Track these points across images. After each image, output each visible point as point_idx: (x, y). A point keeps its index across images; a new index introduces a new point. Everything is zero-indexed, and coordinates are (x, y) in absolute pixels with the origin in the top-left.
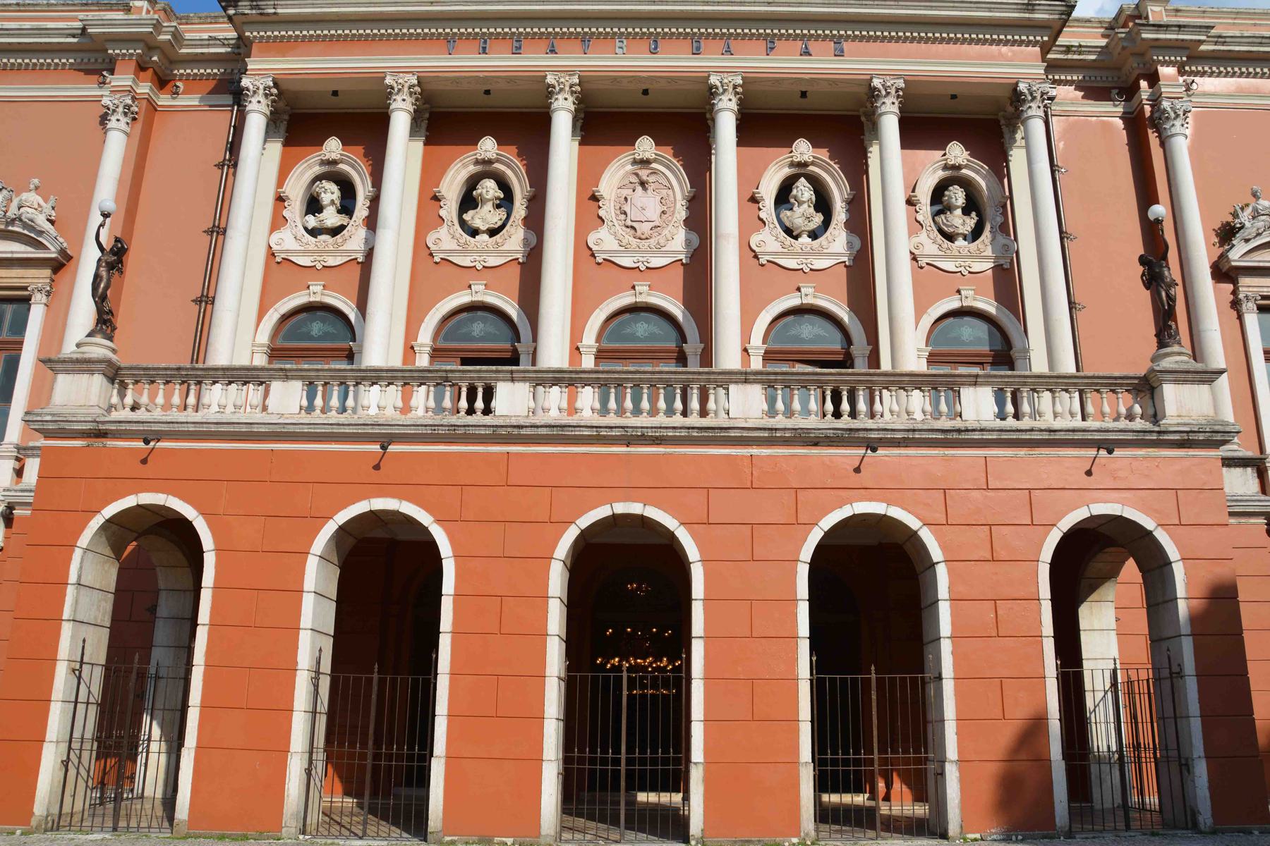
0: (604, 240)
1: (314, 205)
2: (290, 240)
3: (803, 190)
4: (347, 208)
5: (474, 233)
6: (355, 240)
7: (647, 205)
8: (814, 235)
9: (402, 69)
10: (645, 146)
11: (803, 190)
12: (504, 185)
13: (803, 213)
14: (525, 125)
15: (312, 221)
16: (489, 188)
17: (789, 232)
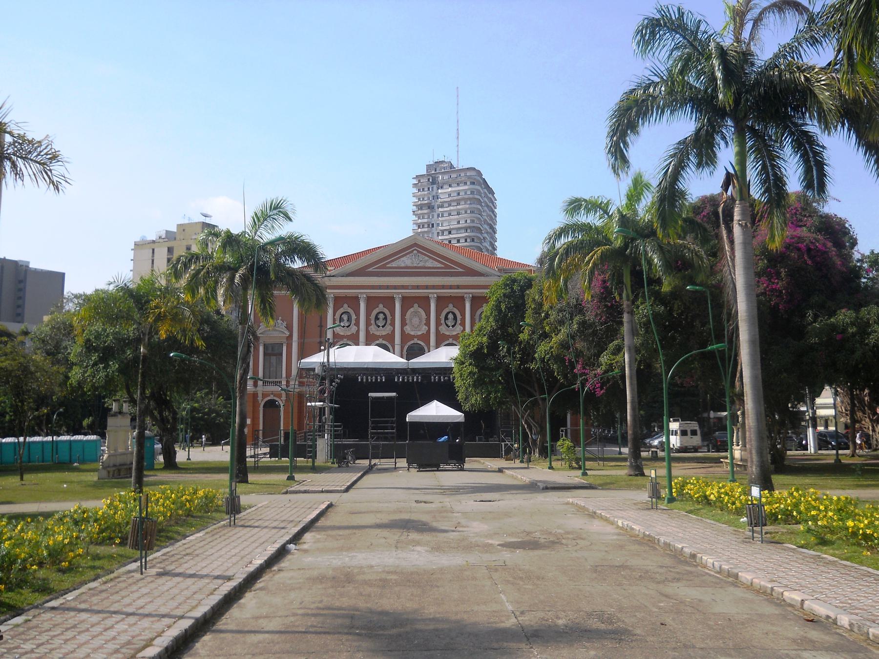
0: (408, 329)
1: (341, 320)
2: (338, 330)
3: (451, 316)
4: (349, 319)
5: (379, 326)
6: (354, 329)
7: (416, 321)
8: (453, 326)
9: (363, 294)
10: (416, 305)
11: (451, 316)
12: (385, 314)
13: (450, 322)
14: (389, 301)
15: (342, 324)
16: (381, 316)
17: (447, 325)
